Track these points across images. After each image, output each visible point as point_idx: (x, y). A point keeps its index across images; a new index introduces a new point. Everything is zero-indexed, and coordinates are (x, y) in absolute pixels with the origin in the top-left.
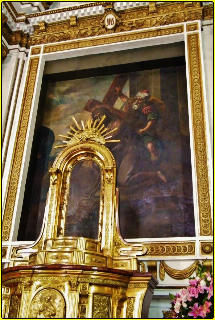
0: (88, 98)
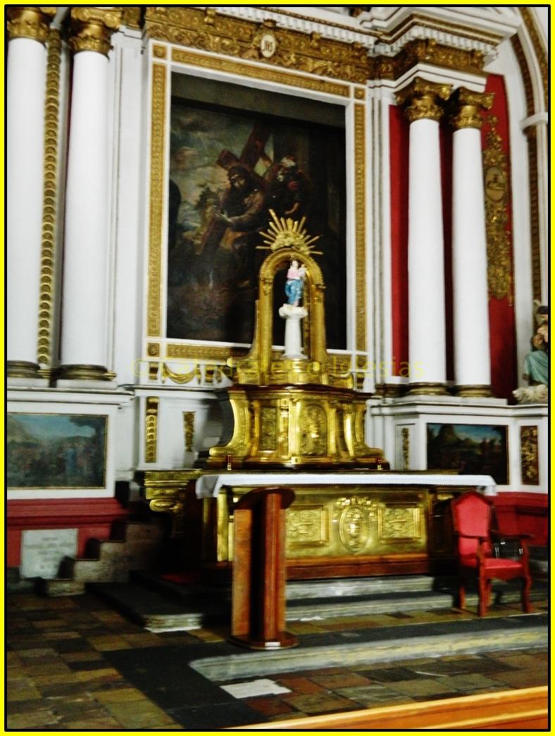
0: (221, 147)
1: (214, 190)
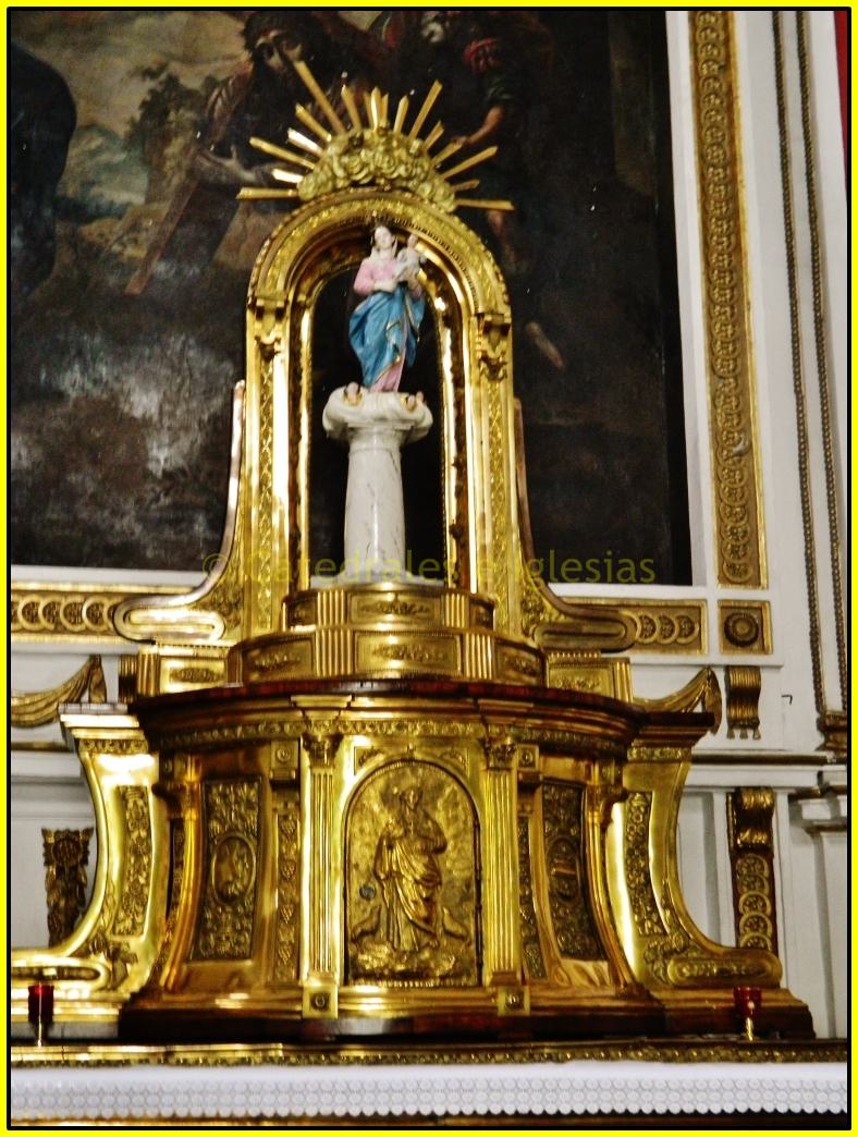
1: (192, 80)
